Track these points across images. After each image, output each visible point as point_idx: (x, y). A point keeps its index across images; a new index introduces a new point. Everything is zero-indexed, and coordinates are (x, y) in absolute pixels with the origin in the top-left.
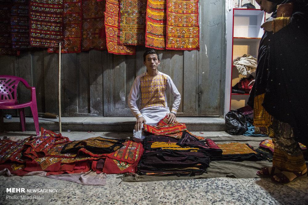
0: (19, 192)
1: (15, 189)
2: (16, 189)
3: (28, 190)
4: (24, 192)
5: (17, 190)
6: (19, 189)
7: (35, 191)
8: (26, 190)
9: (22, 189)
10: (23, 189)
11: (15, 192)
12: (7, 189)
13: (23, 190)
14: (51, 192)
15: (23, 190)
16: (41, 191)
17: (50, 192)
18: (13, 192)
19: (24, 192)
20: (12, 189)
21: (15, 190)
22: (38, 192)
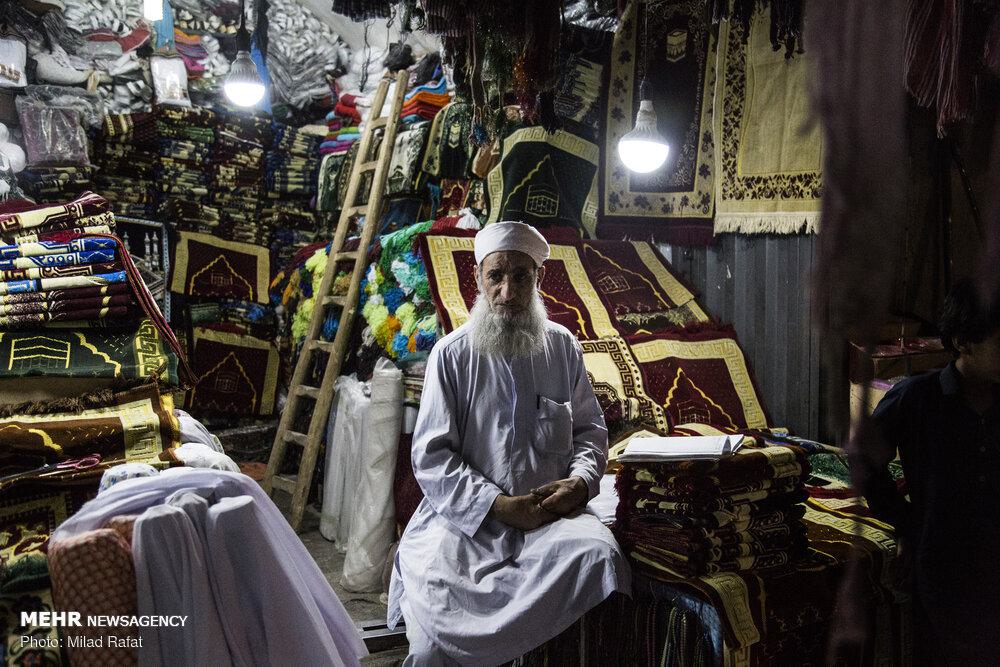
0: (63, 624)
1: (49, 613)
2: (50, 616)
3: (89, 617)
4: (79, 624)
5: (55, 618)
6: (63, 614)
7: (113, 621)
8: (83, 620)
9: (71, 614)
10: (74, 616)
11: (48, 625)
12: (24, 615)
13: (74, 618)
14: (167, 625)
15: (74, 618)
16: (132, 622)
17: (163, 623)
18: (42, 624)
19: (79, 624)
20: (38, 616)
21: (48, 619)
22: (125, 623)
